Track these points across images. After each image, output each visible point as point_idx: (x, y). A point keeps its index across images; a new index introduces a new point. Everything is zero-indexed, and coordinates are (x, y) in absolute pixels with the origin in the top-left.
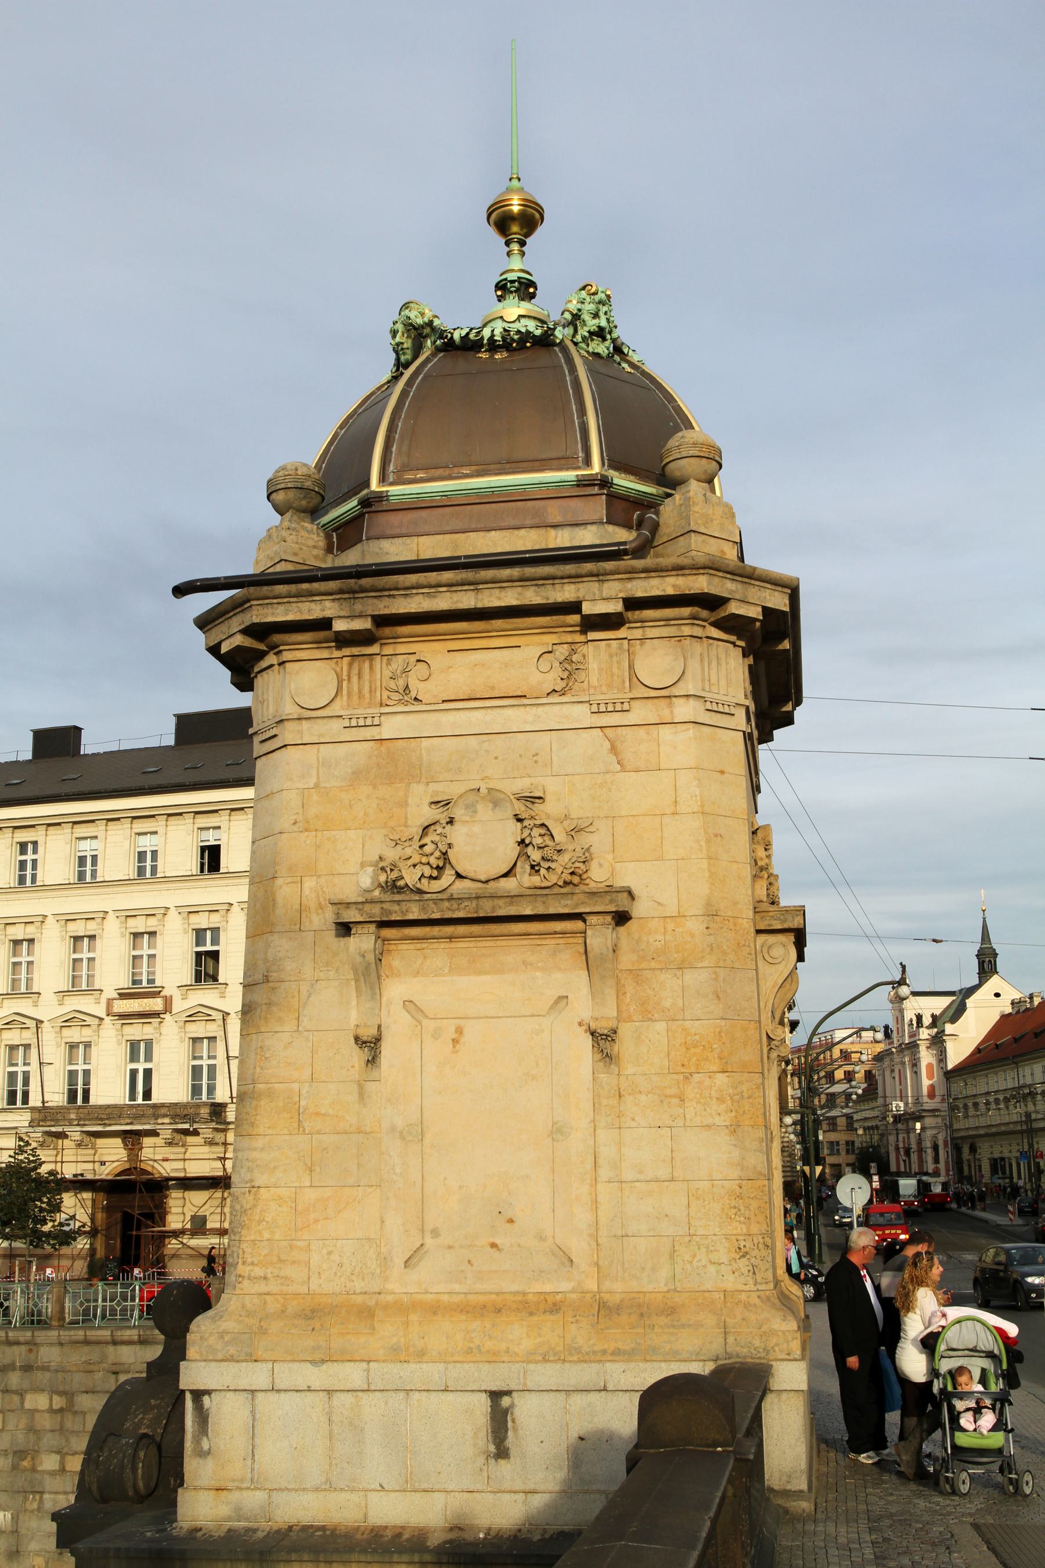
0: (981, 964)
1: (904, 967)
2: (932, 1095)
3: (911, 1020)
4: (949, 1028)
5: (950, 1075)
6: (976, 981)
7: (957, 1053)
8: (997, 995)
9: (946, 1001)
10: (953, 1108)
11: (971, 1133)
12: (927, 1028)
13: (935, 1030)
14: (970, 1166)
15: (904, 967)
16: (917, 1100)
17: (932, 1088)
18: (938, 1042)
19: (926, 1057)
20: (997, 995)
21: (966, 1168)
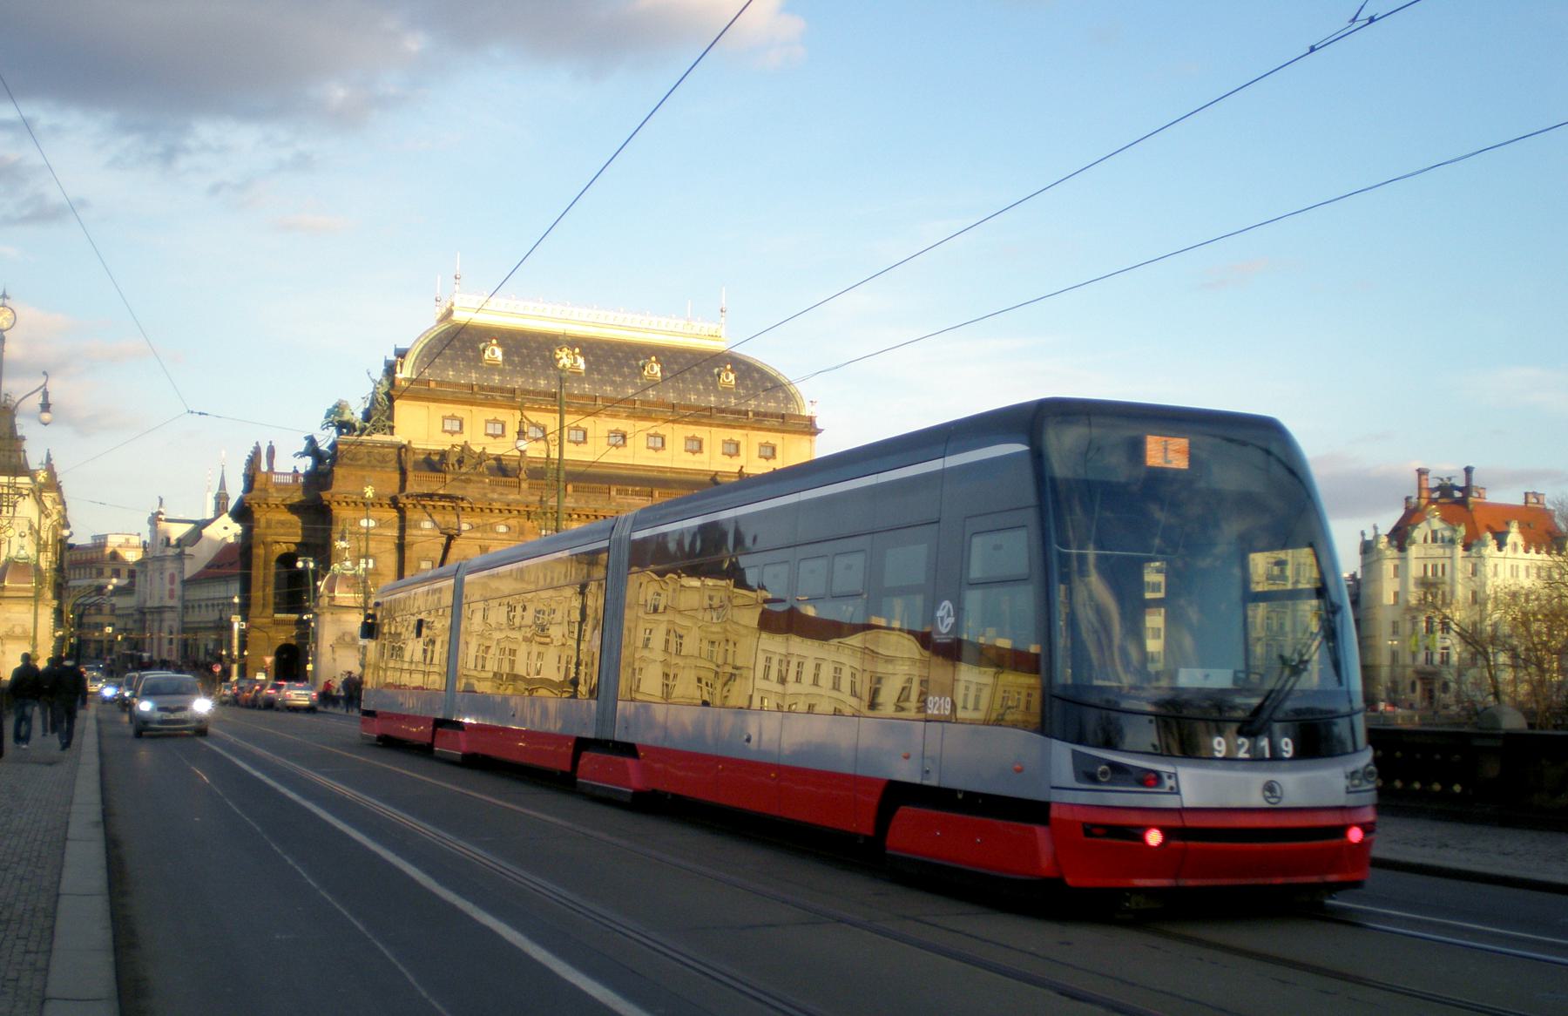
0: (217, 504)
1: (161, 500)
2: (172, 596)
3: (162, 540)
4: (188, 550)
5: (187, 583)
6: (210, 515)
7: (191, 569)
8: (226, 528)
9: (189, 527)
10: (185, 608)
11: (196, 625)
12: (173, 547)
13: (178, 550)
14: (192, 648)
15: (161, 500)
16: (161, 598)
17: (172, 591)
18: (180, 557)
19: (170, 567)
20: (226, 528)
21: (189, 649)
